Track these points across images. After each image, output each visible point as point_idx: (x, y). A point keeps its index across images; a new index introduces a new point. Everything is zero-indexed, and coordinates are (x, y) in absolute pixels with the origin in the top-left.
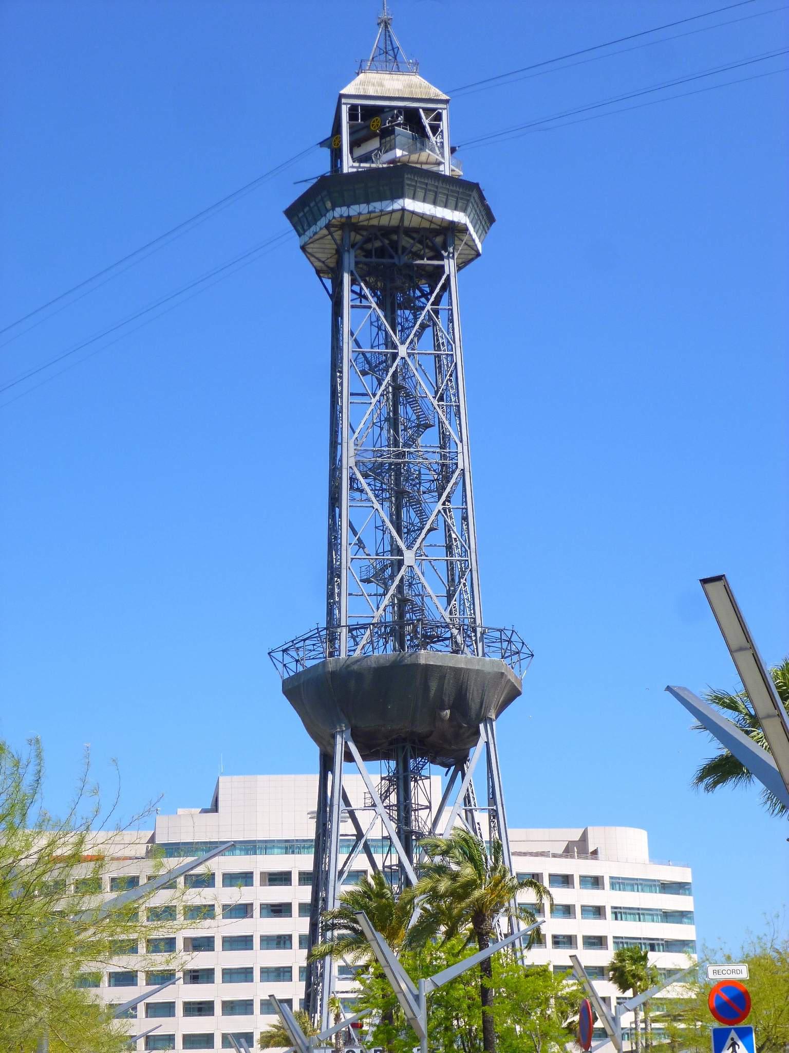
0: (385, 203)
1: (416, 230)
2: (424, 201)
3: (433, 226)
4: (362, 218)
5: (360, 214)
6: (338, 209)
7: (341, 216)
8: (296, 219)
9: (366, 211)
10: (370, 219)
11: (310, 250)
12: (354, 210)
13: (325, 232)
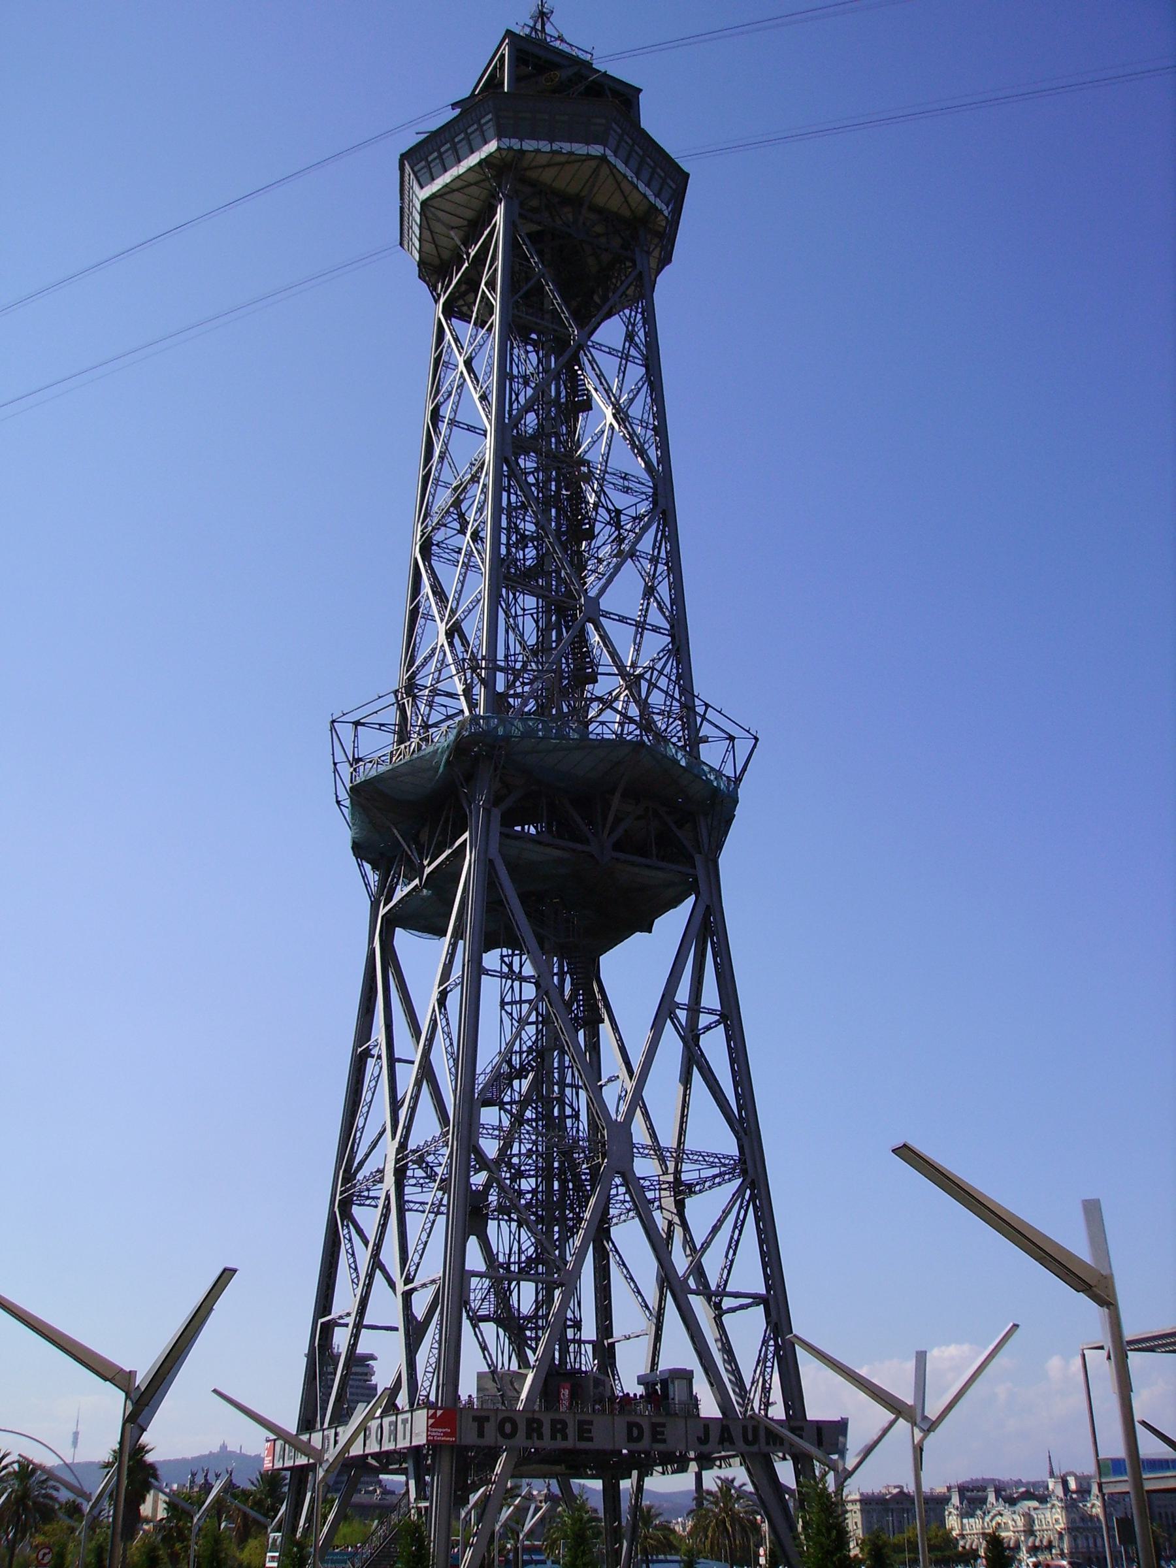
5: (538, 151)
12: (529, 145)
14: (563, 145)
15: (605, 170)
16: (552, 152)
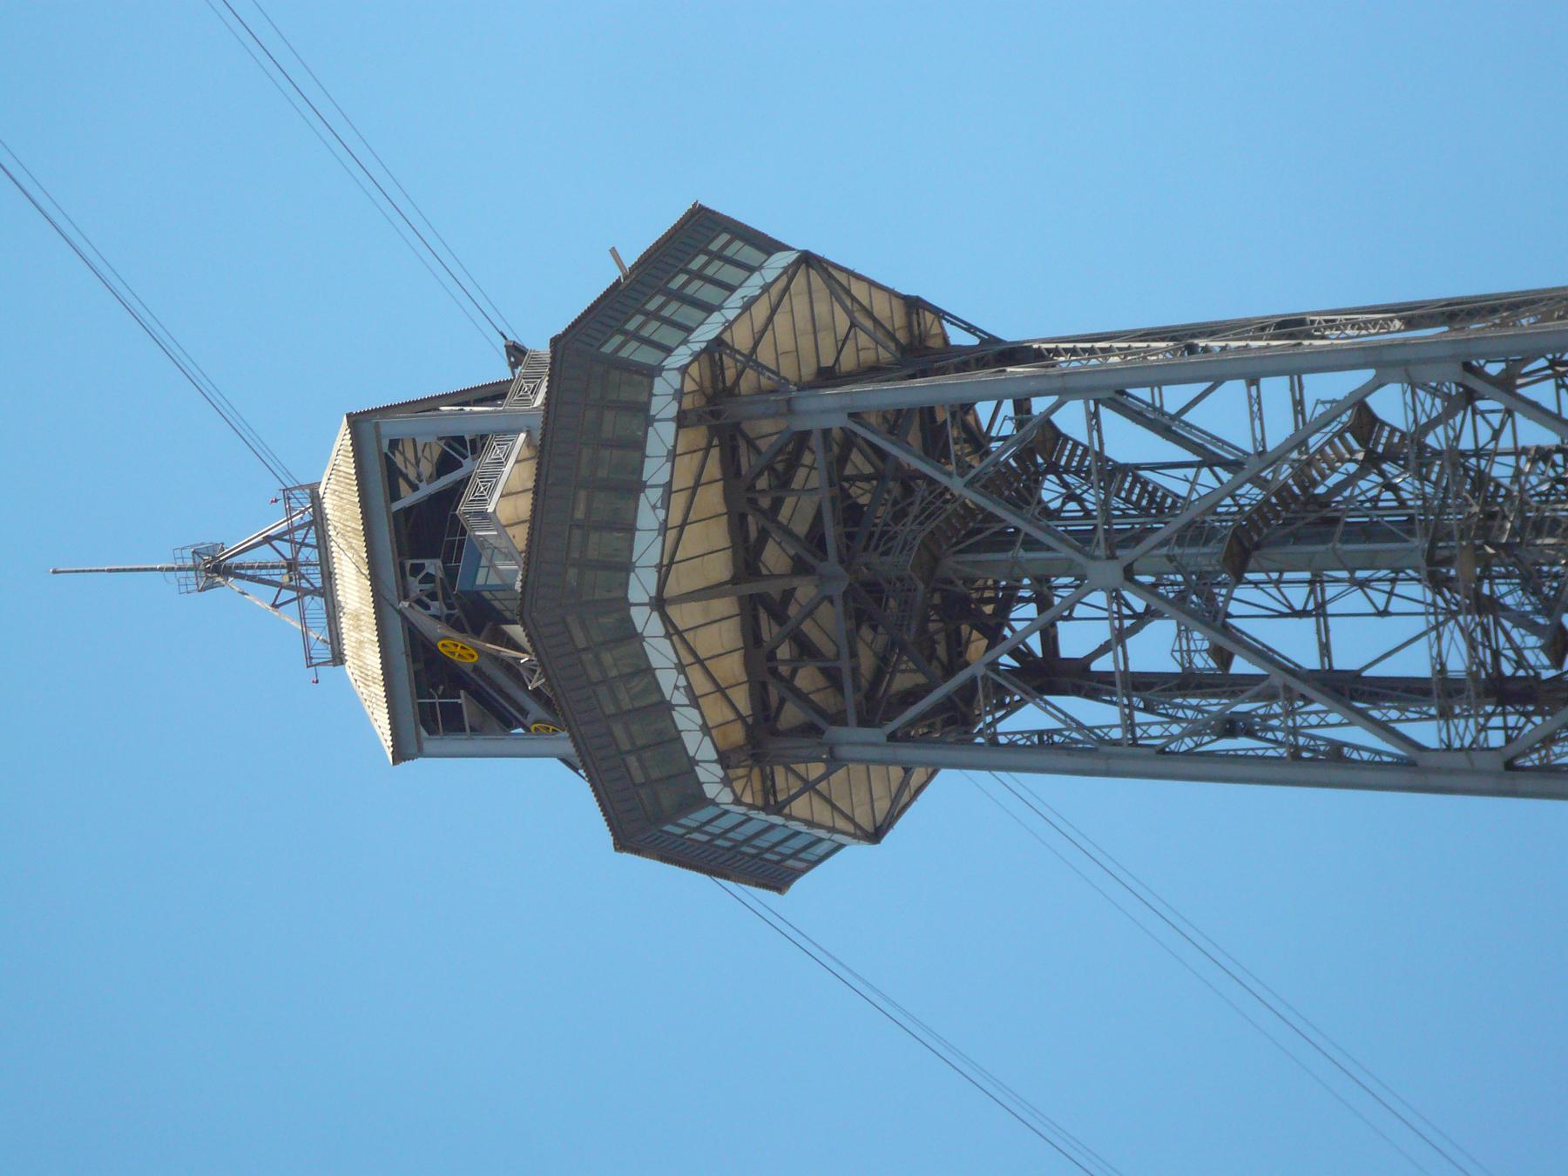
0: (656, 660)
1: (737, 524)
2: (631, 529)
3: (713, 468)
4: (718, 712)
5: (706, 729)
6: (711, 791)
7: (727, 782)
8: (790, 863)
9: (694, 713)
10: (720, 690)
11: (883, 806)
12: (700, 747)
13: (800, 807)
14: (667, 689)
15: (681, 581)
16: (694, 702)
